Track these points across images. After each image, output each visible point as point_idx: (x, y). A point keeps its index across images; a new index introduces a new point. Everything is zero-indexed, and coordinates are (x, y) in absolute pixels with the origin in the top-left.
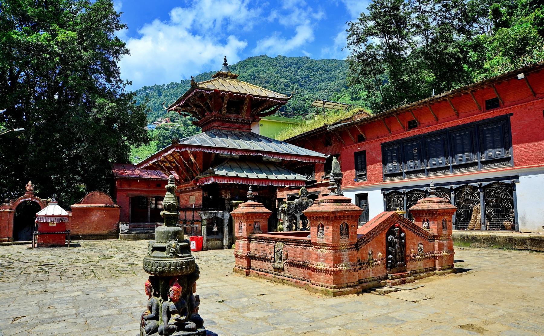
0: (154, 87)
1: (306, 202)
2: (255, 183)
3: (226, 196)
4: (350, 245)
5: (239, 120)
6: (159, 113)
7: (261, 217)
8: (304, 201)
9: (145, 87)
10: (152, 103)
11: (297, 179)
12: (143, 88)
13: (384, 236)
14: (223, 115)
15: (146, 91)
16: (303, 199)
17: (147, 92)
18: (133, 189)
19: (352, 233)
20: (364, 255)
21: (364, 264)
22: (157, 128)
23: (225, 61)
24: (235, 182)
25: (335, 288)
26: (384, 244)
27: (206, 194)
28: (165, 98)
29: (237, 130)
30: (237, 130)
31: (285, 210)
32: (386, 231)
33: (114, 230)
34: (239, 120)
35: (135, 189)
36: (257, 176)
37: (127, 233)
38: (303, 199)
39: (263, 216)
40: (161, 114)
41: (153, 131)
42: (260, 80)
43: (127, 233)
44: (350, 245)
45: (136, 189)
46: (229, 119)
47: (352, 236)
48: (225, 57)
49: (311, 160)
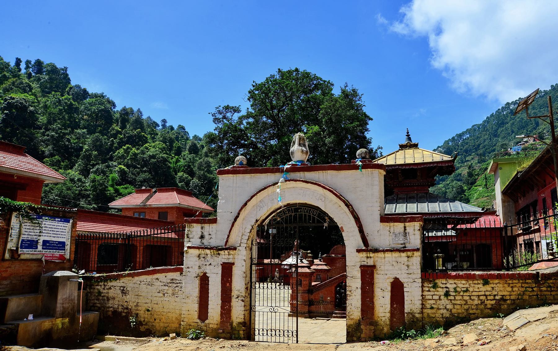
0: (518, 100)
4: (304, 291)
5: (416, 184)
6: (527, 131)
7: (321, 272)
9: (508, 104)
10: (518, 120)
12: (506, 105)
13: (333, 288)
15: (509, 107)
17: (511, 108)
19: (304, 284)
20: (316, 298)
21: (315, 302)
22: (523, 149)
23: (408, 133)
25: (291, 312)
26: (334, 292)
28: (533, 111)
29: (415, 192)
30: (415, 192)
32: (336, 285)
34: (416, 184)
39: (322, 271)
40: (530, 131)
41: (518, 153)
44: (304, 291)
46: (406, 184)
47: (304, 286)
48: (407, 129)
49: (466, 216)
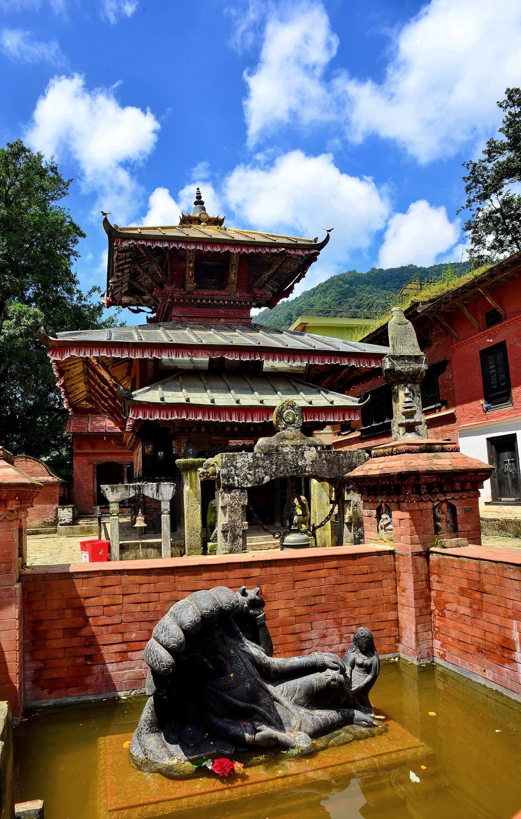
1: (297, 447)
2: (234, 416)
3: (179, 450)
8: (287, 442)
11: (336, 404)
14: (189, 293)
16: (285, 438)
18: (98, 451)
24: (184, 417)
27: (149, 449)
31: (214, 473)
33: (50, 519)
35: (101, 451)
36: (238, 402)
37: (69, 524)
38: (285, 438)
42: (347, 304)
43: (69, 524)
45: (104, 451)
